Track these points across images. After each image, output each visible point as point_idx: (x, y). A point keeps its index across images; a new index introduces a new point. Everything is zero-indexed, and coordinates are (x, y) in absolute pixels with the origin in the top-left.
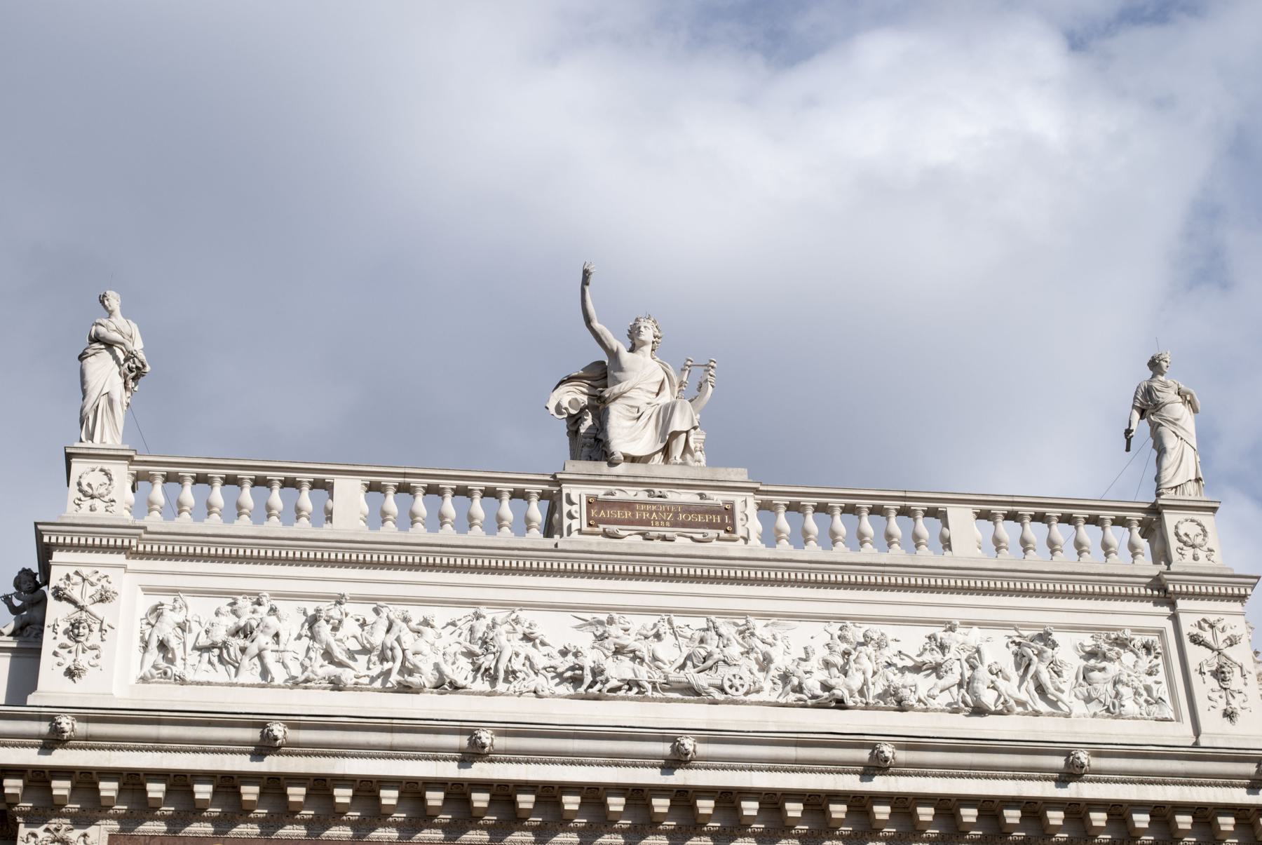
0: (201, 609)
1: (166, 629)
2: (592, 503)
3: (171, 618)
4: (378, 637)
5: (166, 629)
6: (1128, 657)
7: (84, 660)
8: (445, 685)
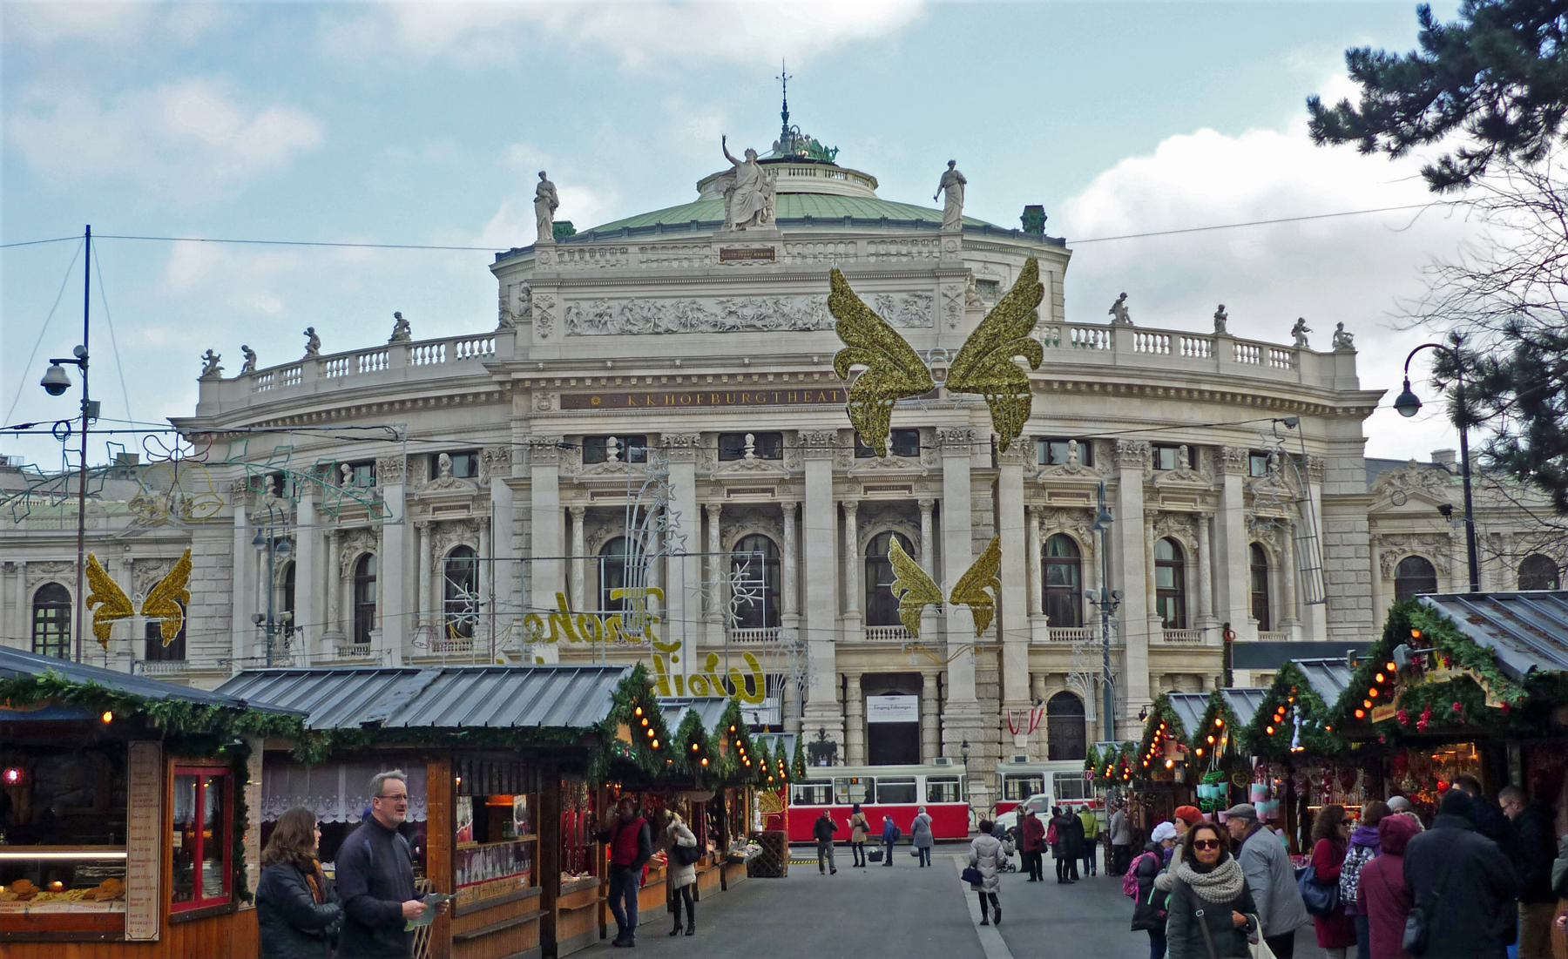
0: (585, 306)
1: (572, 316)
2: (722, 251)
3: (574, 311)
4: (645, 313)
5: (572, 316)
6: (920, 302)
7: (547, 331)
8: (668, 331)
